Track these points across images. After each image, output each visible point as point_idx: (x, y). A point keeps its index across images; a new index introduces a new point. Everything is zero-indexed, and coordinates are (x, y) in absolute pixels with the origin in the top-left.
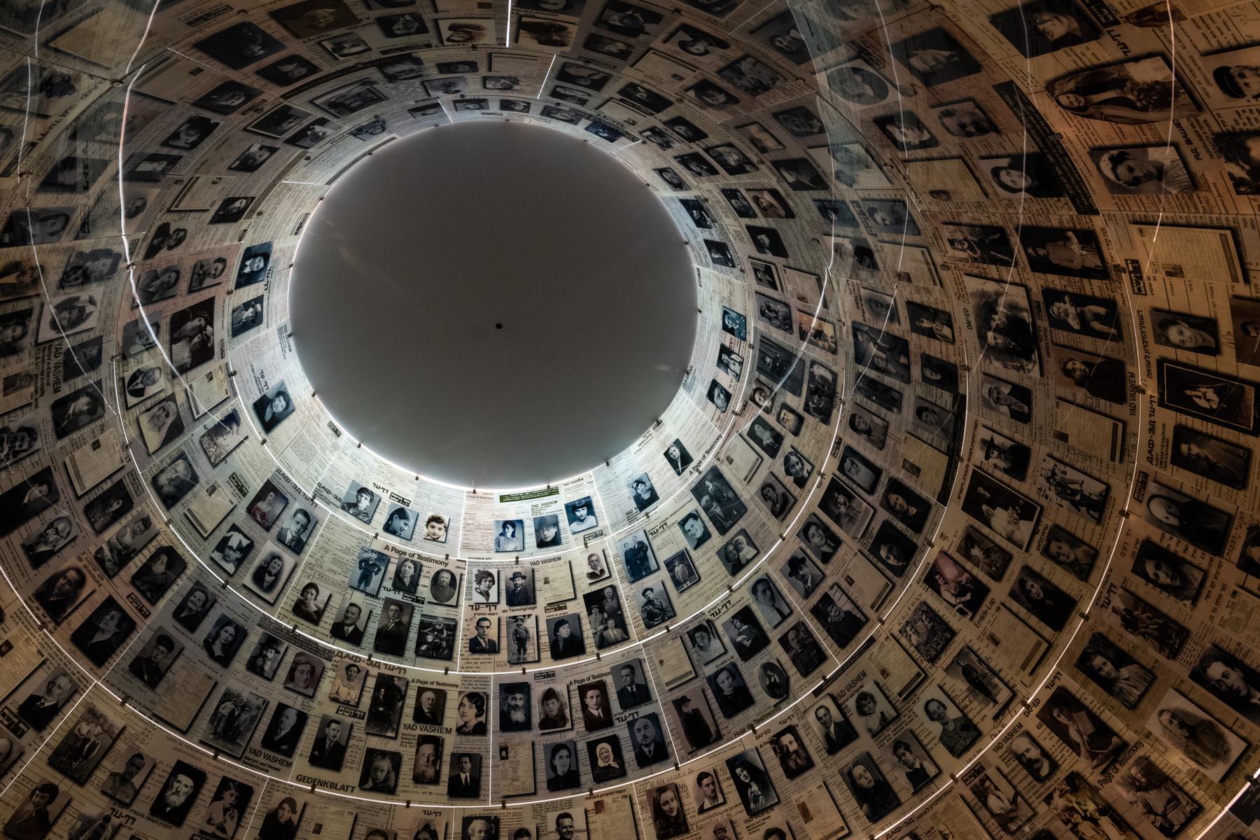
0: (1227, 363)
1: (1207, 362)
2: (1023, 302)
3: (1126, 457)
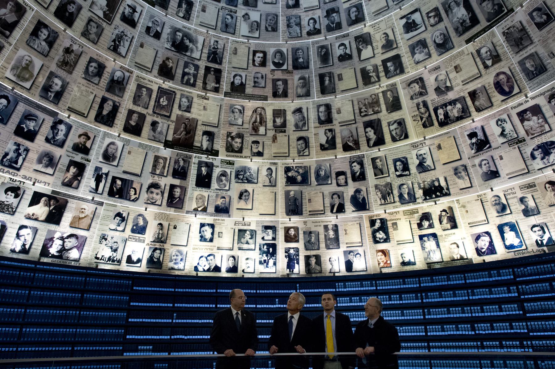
0: (176, 111)
1: (176, 106)
2: (194, 55)
3: (137, 68)
